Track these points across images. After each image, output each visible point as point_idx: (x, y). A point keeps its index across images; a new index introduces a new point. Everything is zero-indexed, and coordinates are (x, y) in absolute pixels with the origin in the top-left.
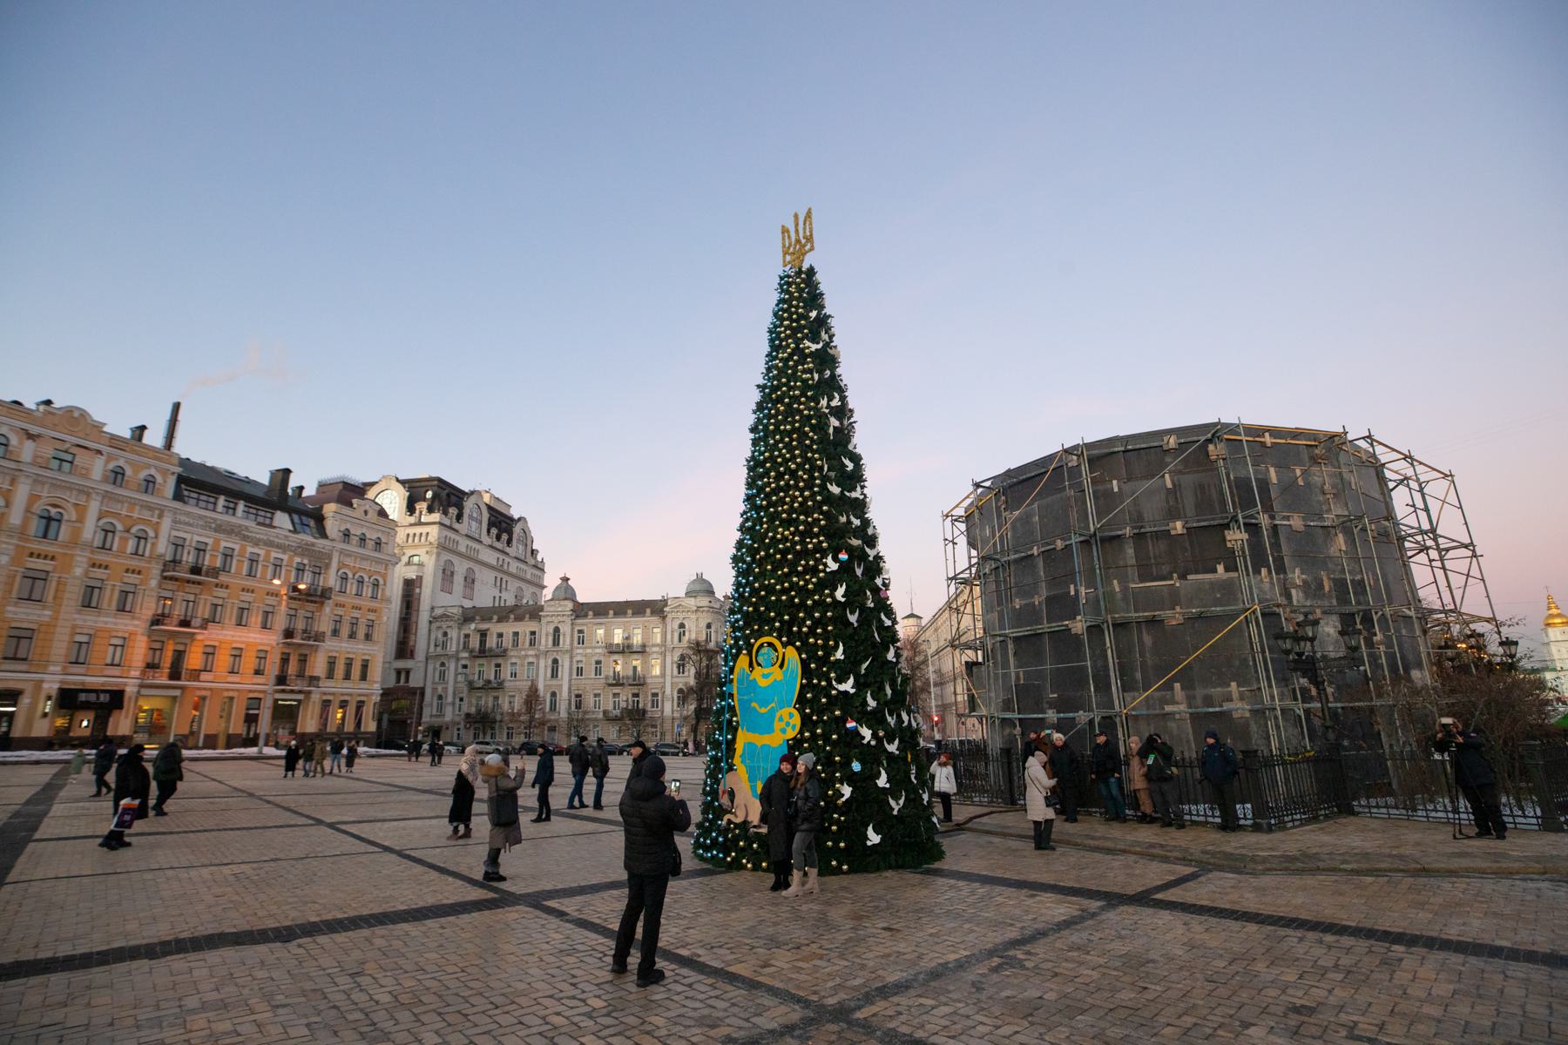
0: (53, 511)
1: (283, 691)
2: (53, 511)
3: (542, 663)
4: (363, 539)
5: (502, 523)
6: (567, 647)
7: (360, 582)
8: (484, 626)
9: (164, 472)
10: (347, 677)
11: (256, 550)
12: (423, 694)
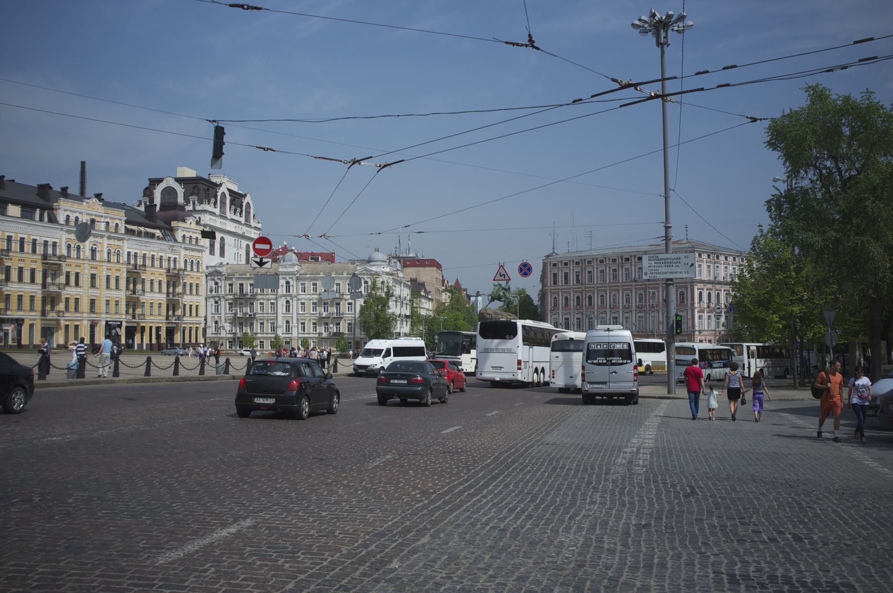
3: (280, 303)
10: (191, 315)
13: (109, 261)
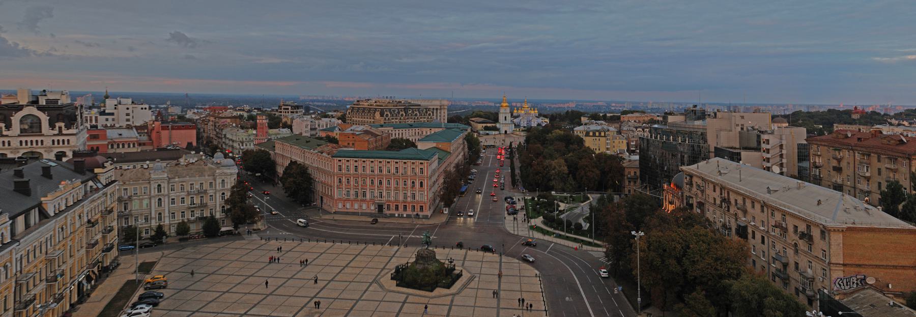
6: (166, 192)
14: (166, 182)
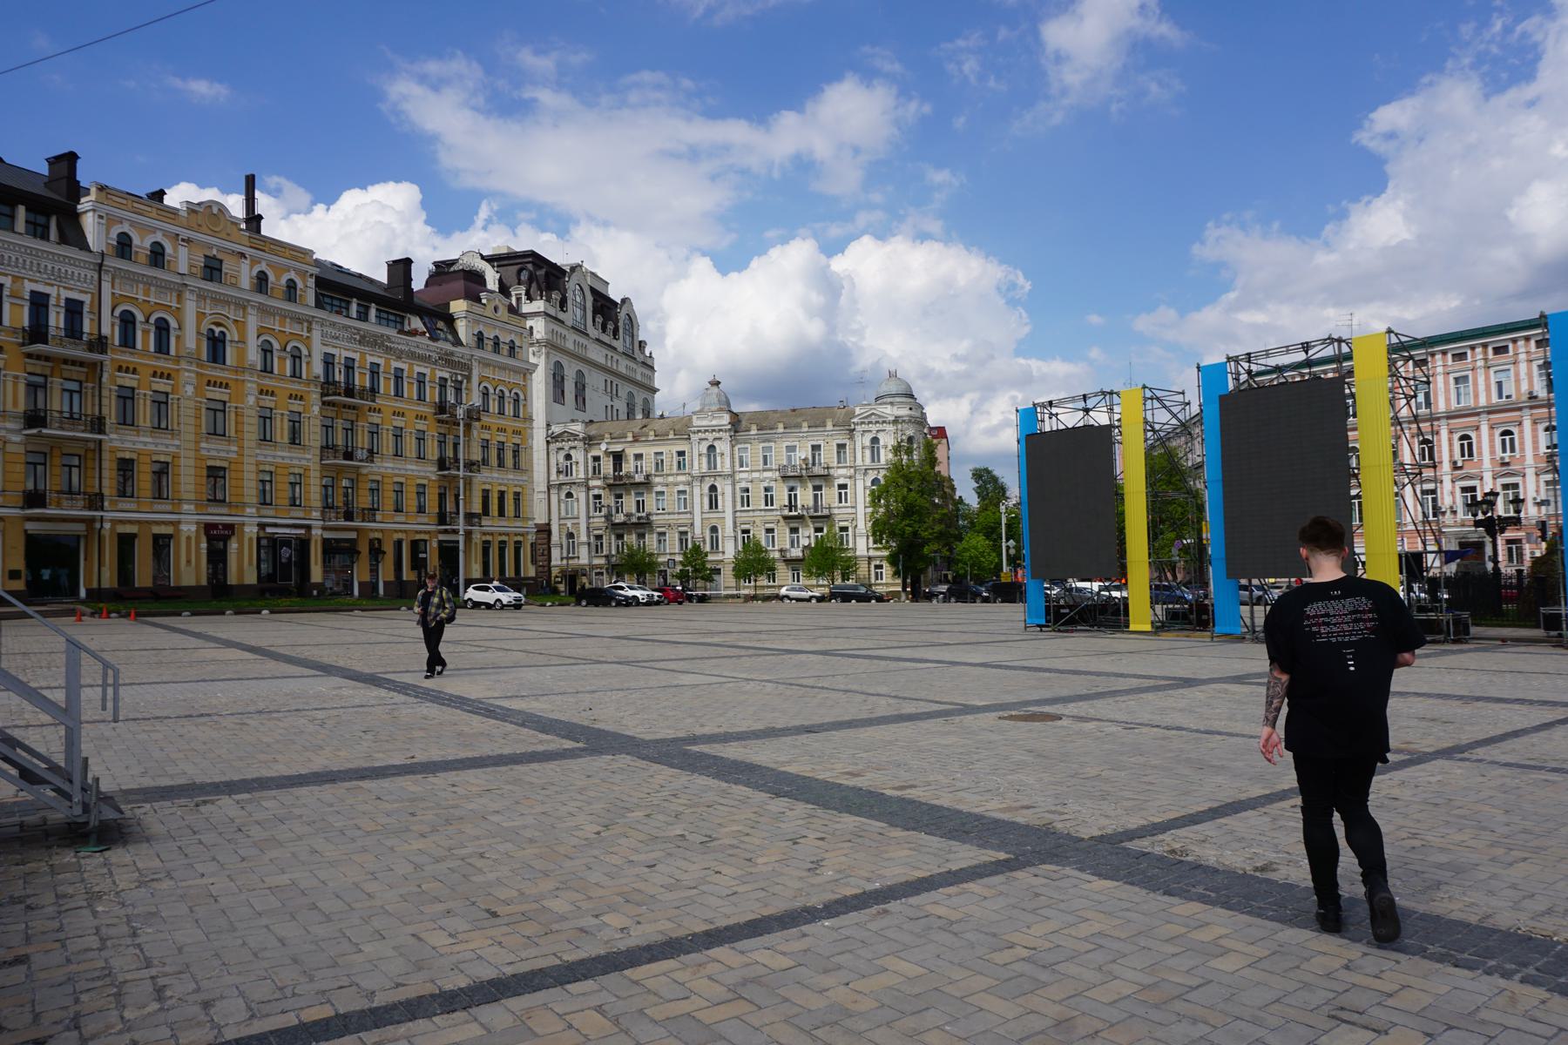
0: (217, 330)
1: (446, 531)
2: (217, 330)
3: (697, 491)
4: (496, 343)
5: (607, 310)
6: (727, 469)
7: (502, 397)
8: (618, 448)
9: (303, 274)
10: (501, 513)
11: (376, 360)
12: (549, 533)
13: (267, 369)
14: (726, 436)
